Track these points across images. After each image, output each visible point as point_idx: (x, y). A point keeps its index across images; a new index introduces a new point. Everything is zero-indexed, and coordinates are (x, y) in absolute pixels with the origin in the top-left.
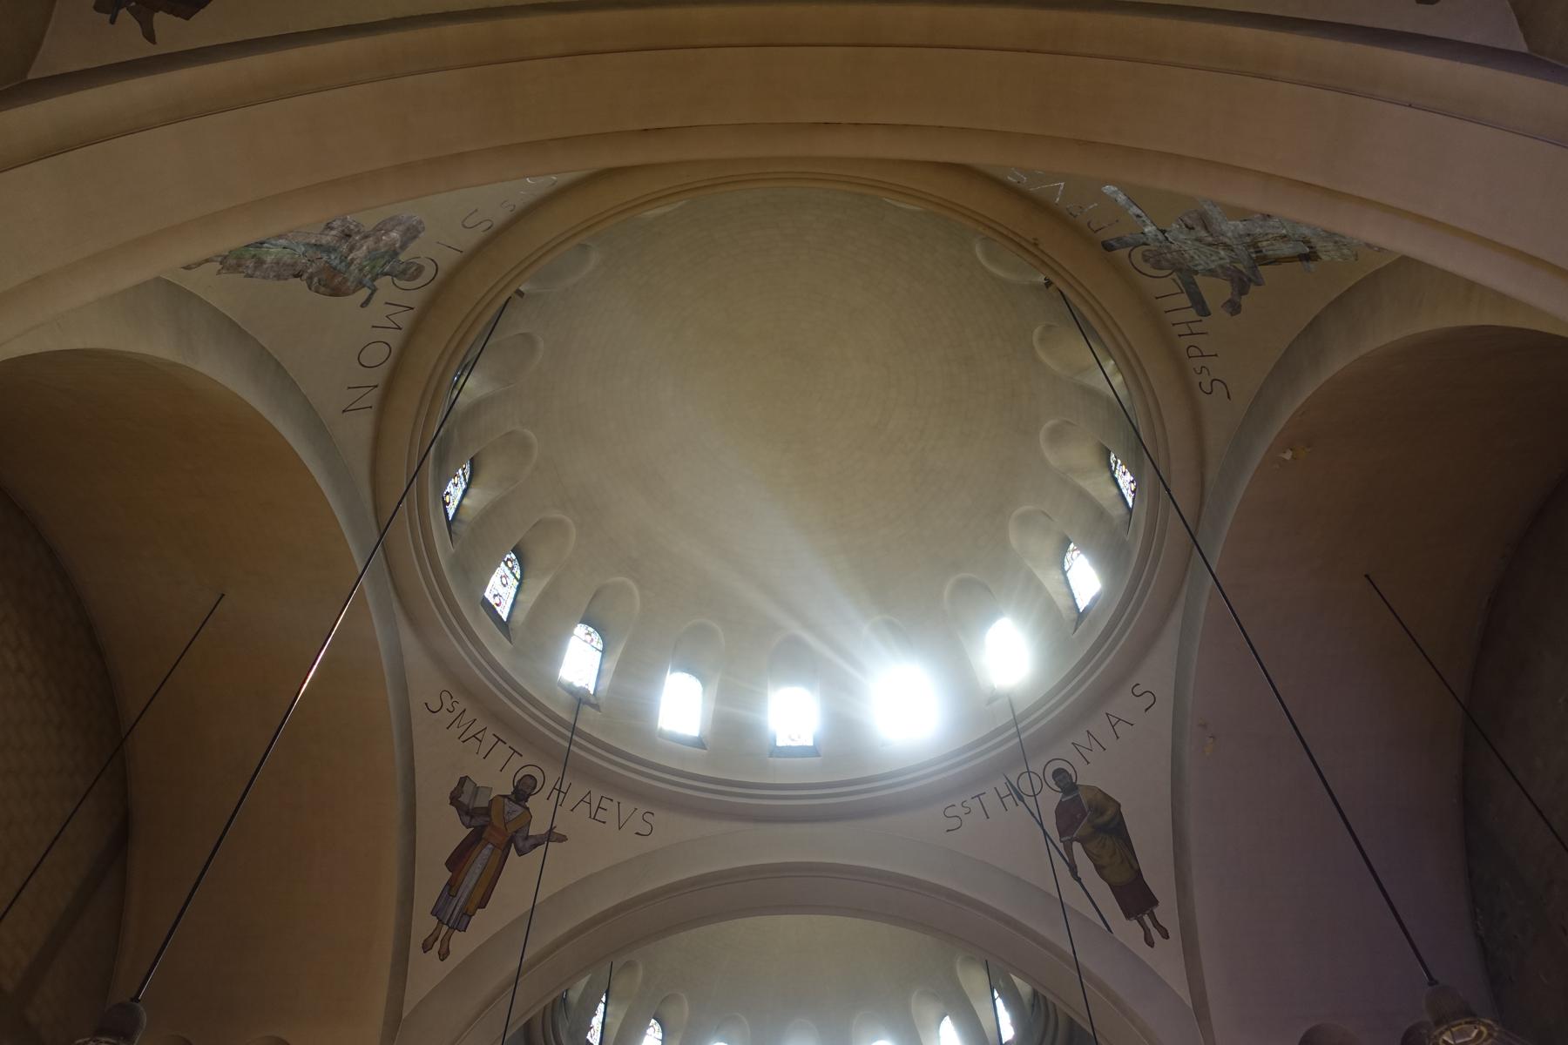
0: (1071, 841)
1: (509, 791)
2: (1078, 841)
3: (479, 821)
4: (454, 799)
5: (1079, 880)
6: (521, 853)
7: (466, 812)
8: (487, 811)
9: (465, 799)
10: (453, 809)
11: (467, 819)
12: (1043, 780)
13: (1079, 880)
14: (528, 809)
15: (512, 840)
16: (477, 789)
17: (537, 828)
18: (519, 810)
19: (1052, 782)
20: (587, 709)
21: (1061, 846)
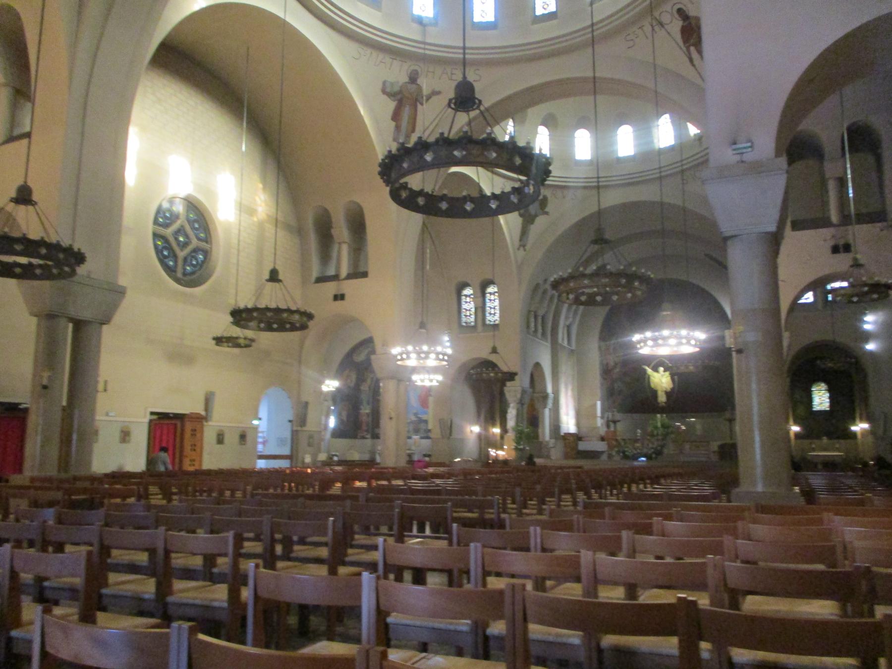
0: (690, 46)
1: (407, 79)
2: (692, 46)
3: (399, 97)
4: (384, 92)
5: (693, 65)
6: (422, 104)
7: (391, 95)
8: (400, 92)
9: (388, 90)
10: (385, 97)
11: (393, 98)
12: (672, 15)
13: (693, 65)
14: (419, 85)
15: (417, 100)
16: (392, 84)
17: (426, 91)
18: (414, 86)
19: (677, 16)
20: (430, 29)
21: (684, 49)
